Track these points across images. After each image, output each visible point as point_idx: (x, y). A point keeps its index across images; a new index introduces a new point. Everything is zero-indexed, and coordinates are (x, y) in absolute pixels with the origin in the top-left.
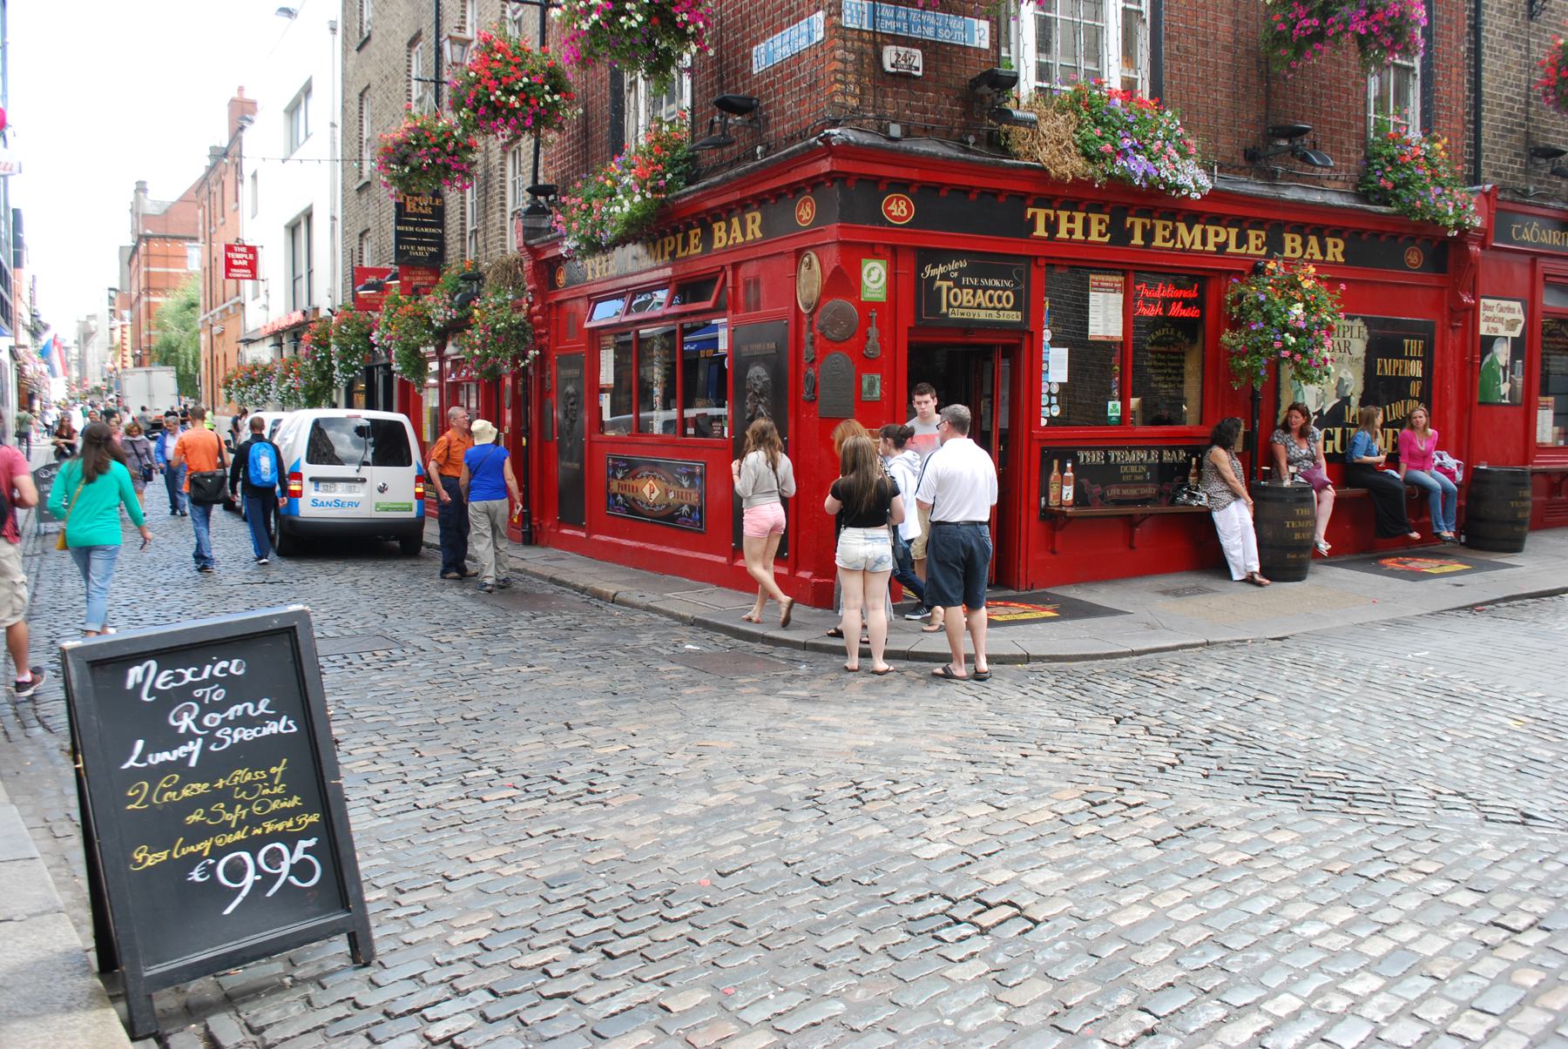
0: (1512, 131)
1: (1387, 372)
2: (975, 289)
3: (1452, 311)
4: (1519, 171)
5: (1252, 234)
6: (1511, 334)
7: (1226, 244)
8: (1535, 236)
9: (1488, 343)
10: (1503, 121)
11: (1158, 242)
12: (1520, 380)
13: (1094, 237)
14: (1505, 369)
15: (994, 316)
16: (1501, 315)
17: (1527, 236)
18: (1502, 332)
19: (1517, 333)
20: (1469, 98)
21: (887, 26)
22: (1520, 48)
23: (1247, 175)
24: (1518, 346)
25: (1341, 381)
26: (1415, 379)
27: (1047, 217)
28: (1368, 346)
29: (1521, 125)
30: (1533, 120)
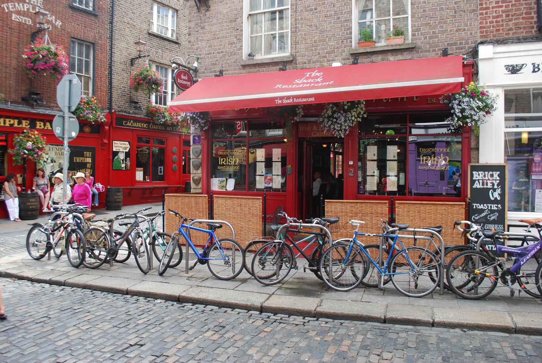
0: (125, 96)
1: (78, 161)
3: (102, 144)
4: (127, 106)
5: (24, 122)
6: (125, 151)
7: (13, 124)
8: (132, 124)
9: (116, 153)
10: (121, 93)
12: (129, 163)
14: (123, 160)
16: (121, 145)
17: (129, 124)
18: (121, 150)
19: (127, 150)
20: (109, 86)
22: (128, 73)
23: (22, 104)
24: (127, 155)
25: (60, 163)
26: (89, 163)
29: (128, 94)
30: (132, 93)
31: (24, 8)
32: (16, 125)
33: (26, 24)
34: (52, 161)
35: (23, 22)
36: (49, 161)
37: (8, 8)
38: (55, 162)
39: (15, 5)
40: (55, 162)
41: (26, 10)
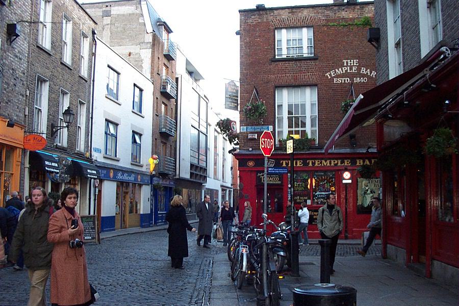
2: (269, 177)
5: (346, 161)
7: (338, 163)
11: (316, 165)
13: (298, 165)
15: (274, 182)
21: (249, 131)
27: (286, 162)
31: (343, 71)
32: (339, 164)
33: (345, 83)
34: (371, 192)
35: (343, 82)
36: (369, 192)
37: (330, 75)
38: (374, 192)
39: (335, 71)
40: (374, 192)
41: (344, 72)
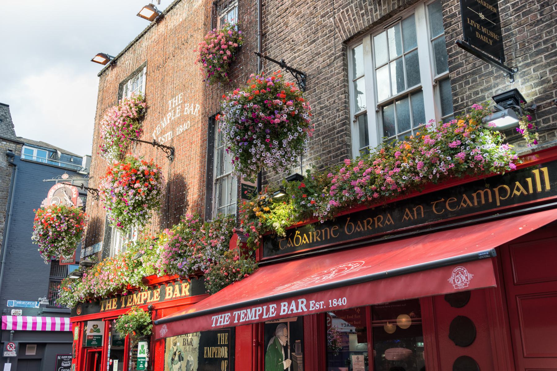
1: (210, 356)
14: (286, 348)
25: (188, 361)
26: (224, 359)
28: (200, 340)
36: (177, 358)
38: (183, 360)
